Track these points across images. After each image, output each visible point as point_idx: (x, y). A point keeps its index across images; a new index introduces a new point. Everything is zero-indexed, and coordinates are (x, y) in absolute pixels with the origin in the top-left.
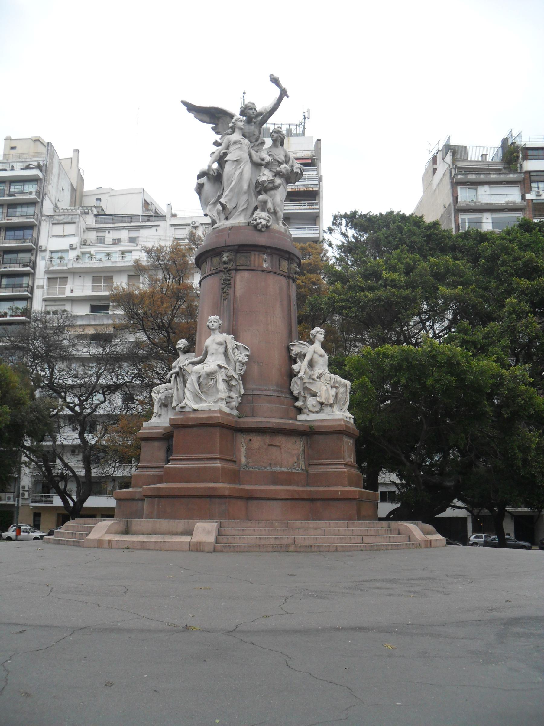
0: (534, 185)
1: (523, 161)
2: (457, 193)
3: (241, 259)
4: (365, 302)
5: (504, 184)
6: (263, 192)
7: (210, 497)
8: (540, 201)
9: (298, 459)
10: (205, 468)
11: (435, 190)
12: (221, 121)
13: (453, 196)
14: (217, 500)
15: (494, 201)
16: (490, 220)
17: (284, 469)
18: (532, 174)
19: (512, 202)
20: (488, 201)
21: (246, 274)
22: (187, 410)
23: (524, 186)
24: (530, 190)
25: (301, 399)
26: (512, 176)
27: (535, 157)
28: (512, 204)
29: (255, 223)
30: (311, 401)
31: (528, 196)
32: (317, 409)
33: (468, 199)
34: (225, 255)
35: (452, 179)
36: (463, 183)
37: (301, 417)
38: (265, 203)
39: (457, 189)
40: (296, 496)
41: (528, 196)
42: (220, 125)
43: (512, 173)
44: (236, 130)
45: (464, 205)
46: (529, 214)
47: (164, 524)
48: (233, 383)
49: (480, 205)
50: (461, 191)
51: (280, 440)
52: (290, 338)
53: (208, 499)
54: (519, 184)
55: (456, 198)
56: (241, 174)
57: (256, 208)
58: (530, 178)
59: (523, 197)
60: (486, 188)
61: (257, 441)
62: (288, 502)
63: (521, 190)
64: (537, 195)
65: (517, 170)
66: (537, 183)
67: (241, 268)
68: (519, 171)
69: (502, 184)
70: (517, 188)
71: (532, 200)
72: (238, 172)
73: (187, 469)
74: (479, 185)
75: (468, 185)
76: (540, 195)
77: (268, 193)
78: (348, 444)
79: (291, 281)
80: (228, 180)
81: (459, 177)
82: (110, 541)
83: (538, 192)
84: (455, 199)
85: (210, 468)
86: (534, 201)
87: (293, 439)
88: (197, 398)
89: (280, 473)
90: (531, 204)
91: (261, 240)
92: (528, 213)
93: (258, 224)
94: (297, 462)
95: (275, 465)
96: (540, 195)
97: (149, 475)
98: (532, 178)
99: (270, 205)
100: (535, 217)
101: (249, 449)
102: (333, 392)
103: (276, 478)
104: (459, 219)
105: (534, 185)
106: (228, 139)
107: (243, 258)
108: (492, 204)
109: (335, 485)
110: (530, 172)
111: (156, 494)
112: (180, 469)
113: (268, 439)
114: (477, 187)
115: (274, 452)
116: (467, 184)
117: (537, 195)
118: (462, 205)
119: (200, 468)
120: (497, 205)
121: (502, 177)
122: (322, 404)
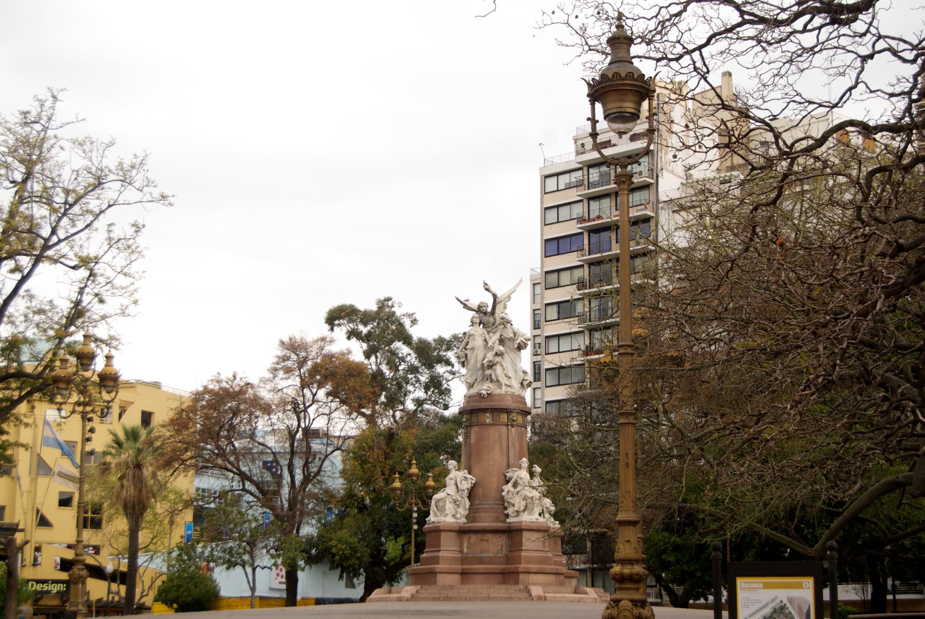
3: (474, 419)
9: (502, 547)
17: (491, 555)
32: (515, 515)
34: (465, 416)
37: (508, 520)
40: (490, 571)
48: (458, 503)
51: (489, 537)
52: (508, 466)
56: (476, 357)
61: (474, 538)
62: (486, 575)
72: (474, 355)
79: (510, 427)
87: (497, 536)
89: (487, 557)
91: (483, 405)
94: (501, 550)
95: (485, 552)
99: (493, 377)
101: (469, 543)
102: (523, 503)
103: (481, 561)
113: (480, 536)
115: (485, 544)
122: (517, 511)
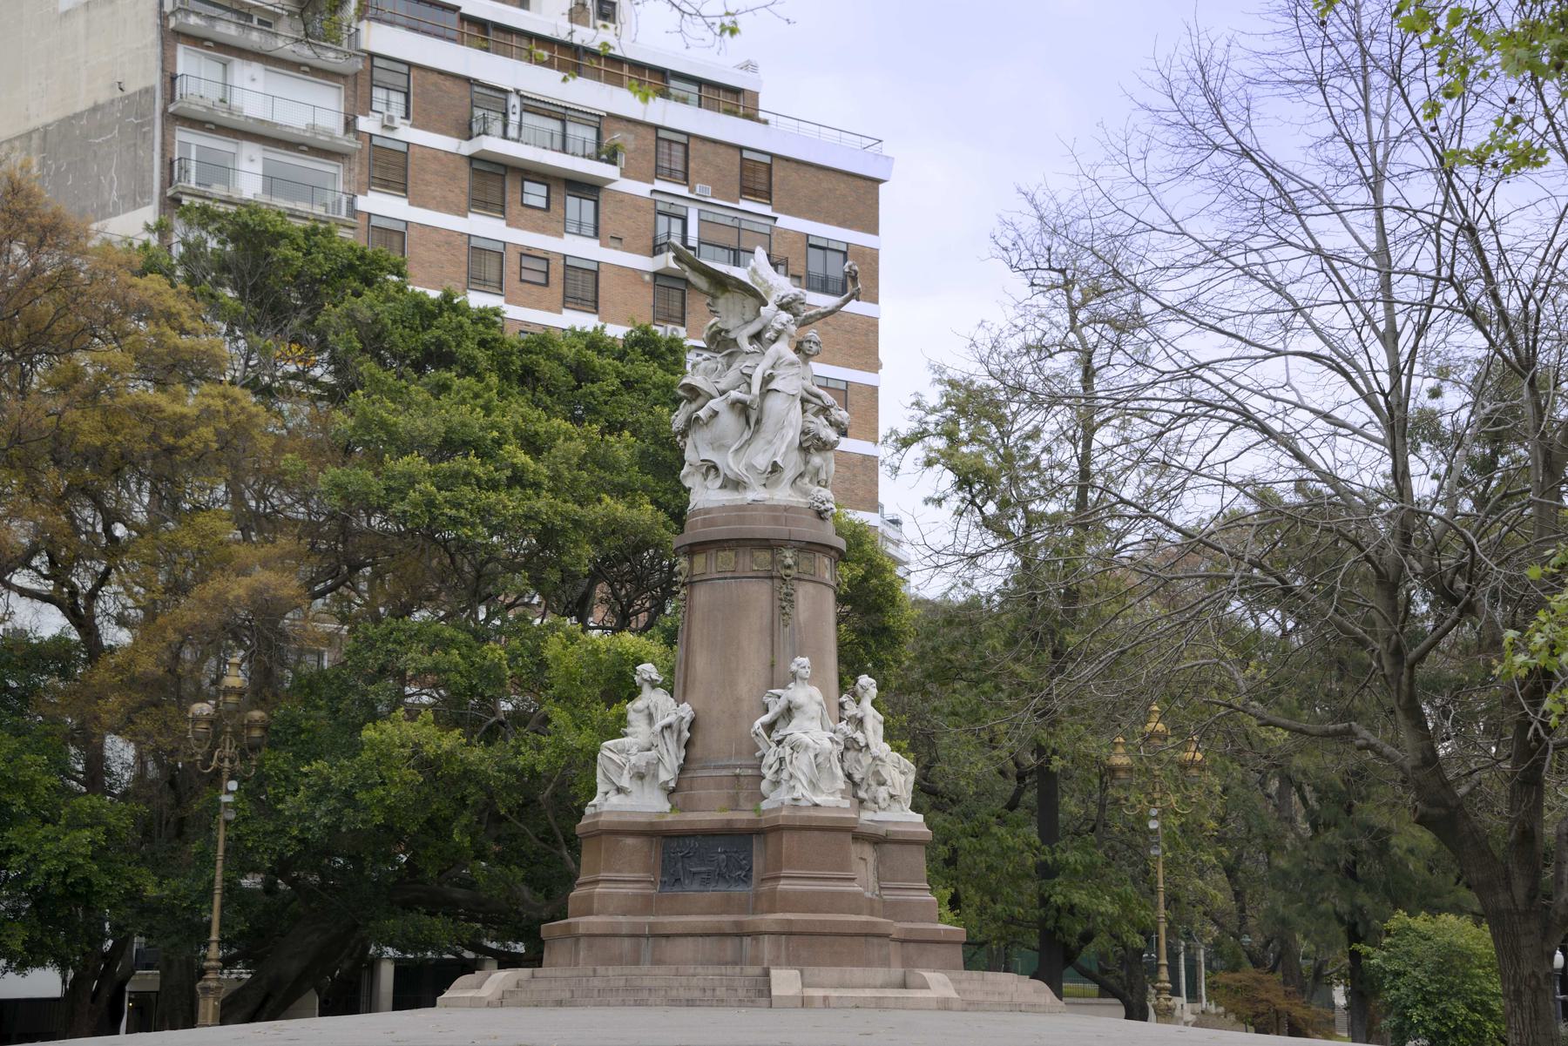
0: (379, 94)
1: (360, 19)
2: (174, 64)
4: (506, 519)
5: (305, 73)
6: (812, 450)
7: (866, 935)
8: (389, 144)
10: (842, 893)
11: (66, 13)
12: (727, 295)
13: (163, 70)
14: (875, 940)
15: (278, 119)
16: (258, 168)
18: (377, 62)
19: (326, 132)
20: (260, 115)
21: (809, 587)
22: (803, 803)
23: (355, 92)
24: (368, 108)
25: (864, 786)
26: (330, 59)
27: (387, 17)
28: (327, 139)
29: (823, 508)
30: (882, 792)
31: (366, 124)
33: (213, 93)
35: (164, 17)
36: (196, 40)
38: (817, 472)
39: (175, 49)
41: (366, 124)
42: (721, 301)
43: (335, 50)
44: (785, 337)
45: (199, 108)
46: (360, 174)
47: (857, 973)
49: (242, 119)
50: (187, 61)
53: (863, 939)
54: (342, 80)
55: (171, 79)
57: (801, 475)
58: (372, 71)
59: (350, 125)
60: (256, 69)
63: (346, 98)
64: (384, 127)
65: (339, 43)
66: (385, 91)
67: (806, 577)
68: (345, 46)
69: (299, 71)
70: (335, 91)
71: (371, 135)
73: (814, 893)
74: (239, 56)
75: (208, 48)
76: (393, 129)
77: (823, 453)
78: (918, 859)
80: (777, 423)
81: (193, 20)
82: (826, 998)
83: (391, 118)
84: (168, 79)
85: (849, 893)
86: (376, 141)
88: (814, 785)
90: (367, 145)
92: (357, 170)
93: (826, 511)
96: (393, 129)
97: (626, 895)
98: (377, 74)
99: (823, 476)
100: (374, 185)
104: (173, 144)
105: (379, 94)
106: (777, 351)
107: (806, 562)
108: (276, 124)
109: (922, 921)
110: (372, 55)
111: (786, 930)
112: (804, 893)
114: (230, 61)
116: (207, 43)
117: (384, 127)
118: (193, 107)
119: (833, 893)
120: (287, 129)
121: (305, 53)
122: (892, 796)
